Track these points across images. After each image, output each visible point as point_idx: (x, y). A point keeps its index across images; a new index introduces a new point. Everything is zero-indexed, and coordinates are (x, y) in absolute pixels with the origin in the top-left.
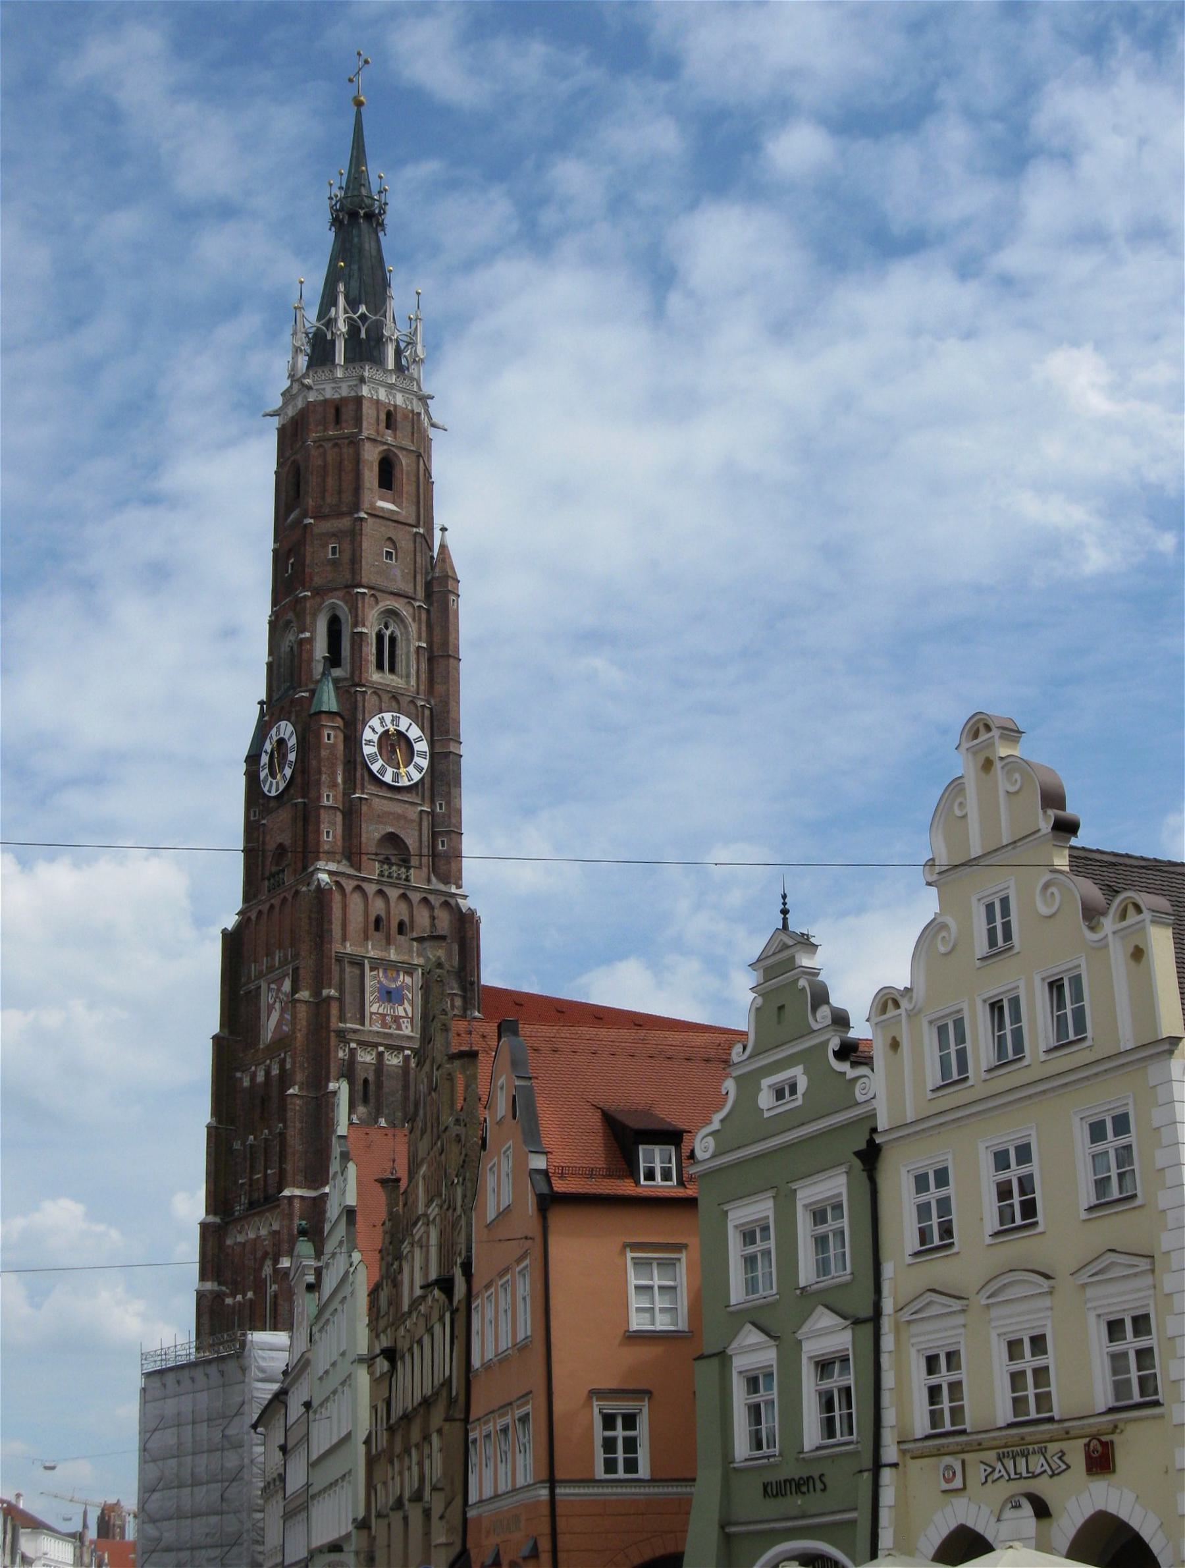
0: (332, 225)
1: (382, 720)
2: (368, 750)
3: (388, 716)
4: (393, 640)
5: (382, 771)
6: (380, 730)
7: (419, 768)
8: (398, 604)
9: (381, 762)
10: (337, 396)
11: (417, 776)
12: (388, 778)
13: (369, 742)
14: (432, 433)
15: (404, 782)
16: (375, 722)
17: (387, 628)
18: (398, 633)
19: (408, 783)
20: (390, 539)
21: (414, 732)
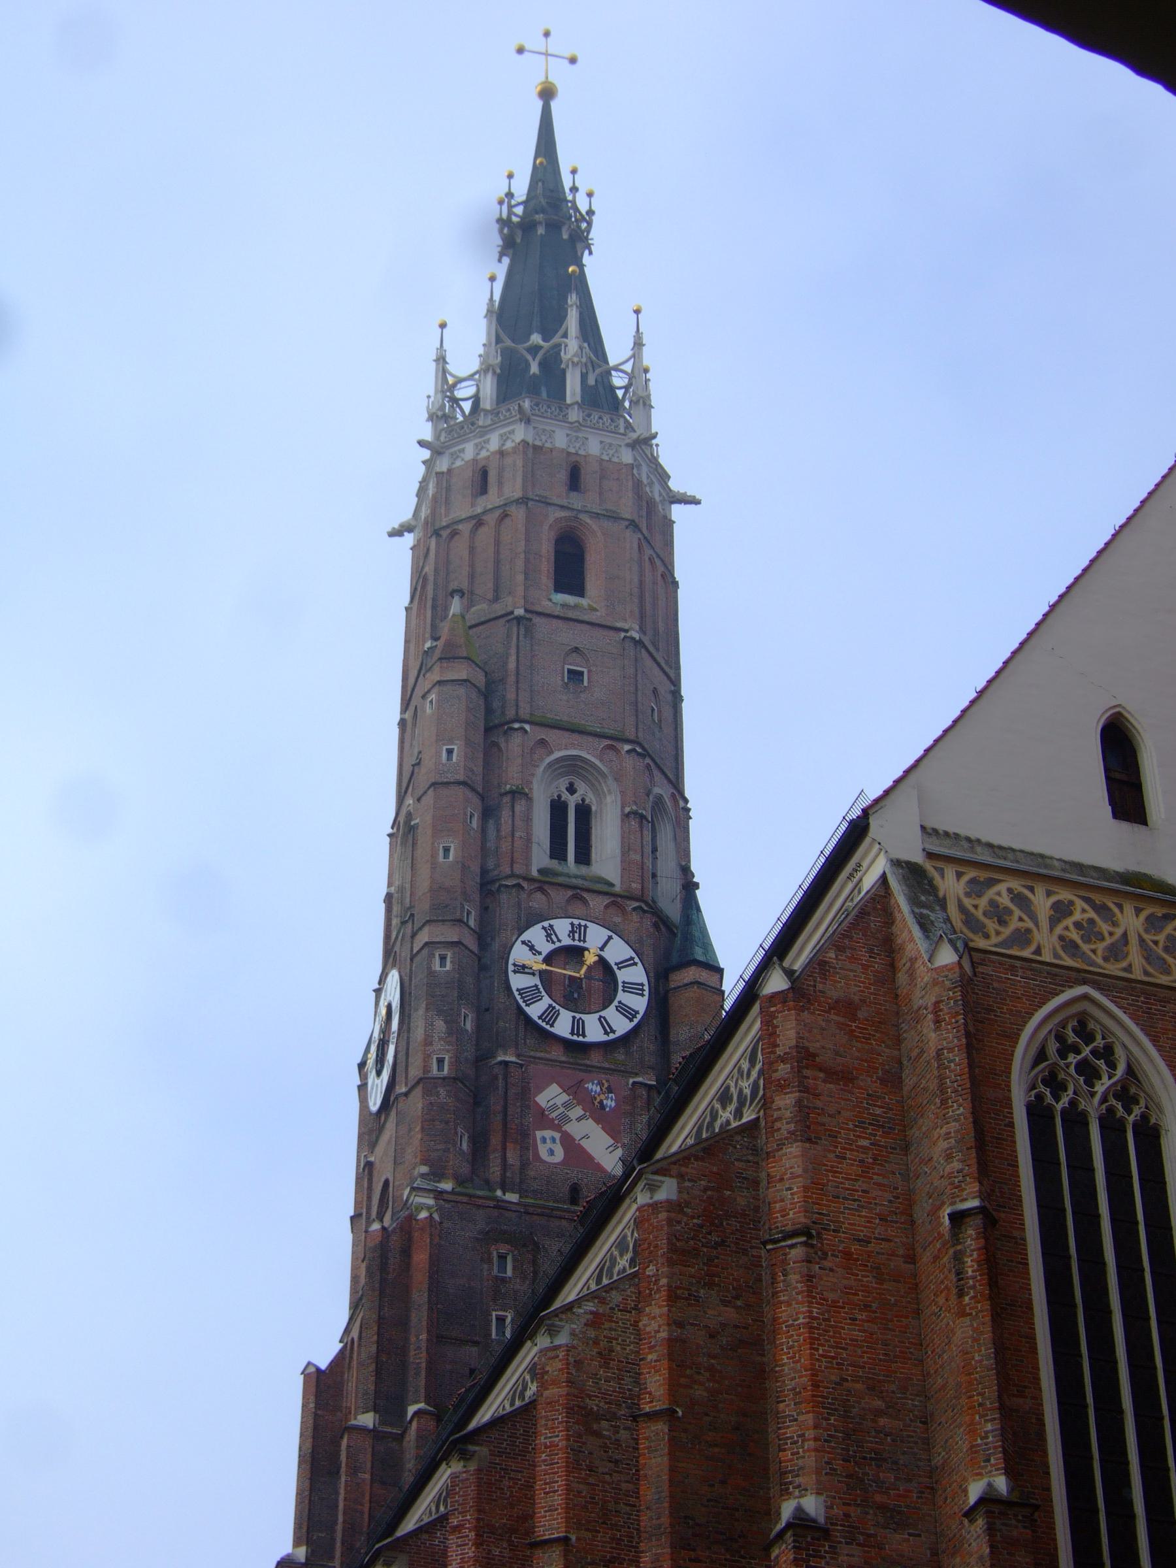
0: (502, 254)
1: (550, 933)
2: (518, 982)
3: (562, 926)
4: (584, 812)
5: (550, 1015)
6: (546, 948)
7: (627, 1012)
8: (586, 751)
9: (546, 1001)
10: (484, 454)
11: (622, 1026)
12: (563, 1027)
13: (522, 969)
14: (678, 512)
15: (594, 1033)
16: (535, 934)
17: (571, 790)
18: (591, 799)
19: (605, 1038)
20: (576, 650)
21: (618, 951)
